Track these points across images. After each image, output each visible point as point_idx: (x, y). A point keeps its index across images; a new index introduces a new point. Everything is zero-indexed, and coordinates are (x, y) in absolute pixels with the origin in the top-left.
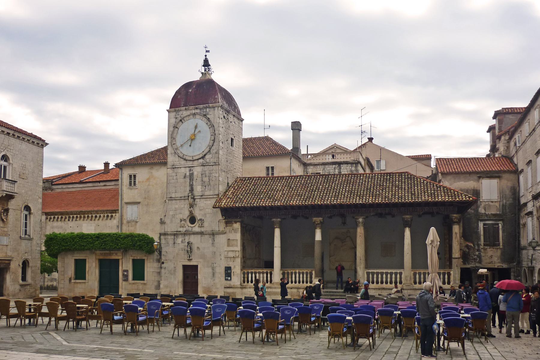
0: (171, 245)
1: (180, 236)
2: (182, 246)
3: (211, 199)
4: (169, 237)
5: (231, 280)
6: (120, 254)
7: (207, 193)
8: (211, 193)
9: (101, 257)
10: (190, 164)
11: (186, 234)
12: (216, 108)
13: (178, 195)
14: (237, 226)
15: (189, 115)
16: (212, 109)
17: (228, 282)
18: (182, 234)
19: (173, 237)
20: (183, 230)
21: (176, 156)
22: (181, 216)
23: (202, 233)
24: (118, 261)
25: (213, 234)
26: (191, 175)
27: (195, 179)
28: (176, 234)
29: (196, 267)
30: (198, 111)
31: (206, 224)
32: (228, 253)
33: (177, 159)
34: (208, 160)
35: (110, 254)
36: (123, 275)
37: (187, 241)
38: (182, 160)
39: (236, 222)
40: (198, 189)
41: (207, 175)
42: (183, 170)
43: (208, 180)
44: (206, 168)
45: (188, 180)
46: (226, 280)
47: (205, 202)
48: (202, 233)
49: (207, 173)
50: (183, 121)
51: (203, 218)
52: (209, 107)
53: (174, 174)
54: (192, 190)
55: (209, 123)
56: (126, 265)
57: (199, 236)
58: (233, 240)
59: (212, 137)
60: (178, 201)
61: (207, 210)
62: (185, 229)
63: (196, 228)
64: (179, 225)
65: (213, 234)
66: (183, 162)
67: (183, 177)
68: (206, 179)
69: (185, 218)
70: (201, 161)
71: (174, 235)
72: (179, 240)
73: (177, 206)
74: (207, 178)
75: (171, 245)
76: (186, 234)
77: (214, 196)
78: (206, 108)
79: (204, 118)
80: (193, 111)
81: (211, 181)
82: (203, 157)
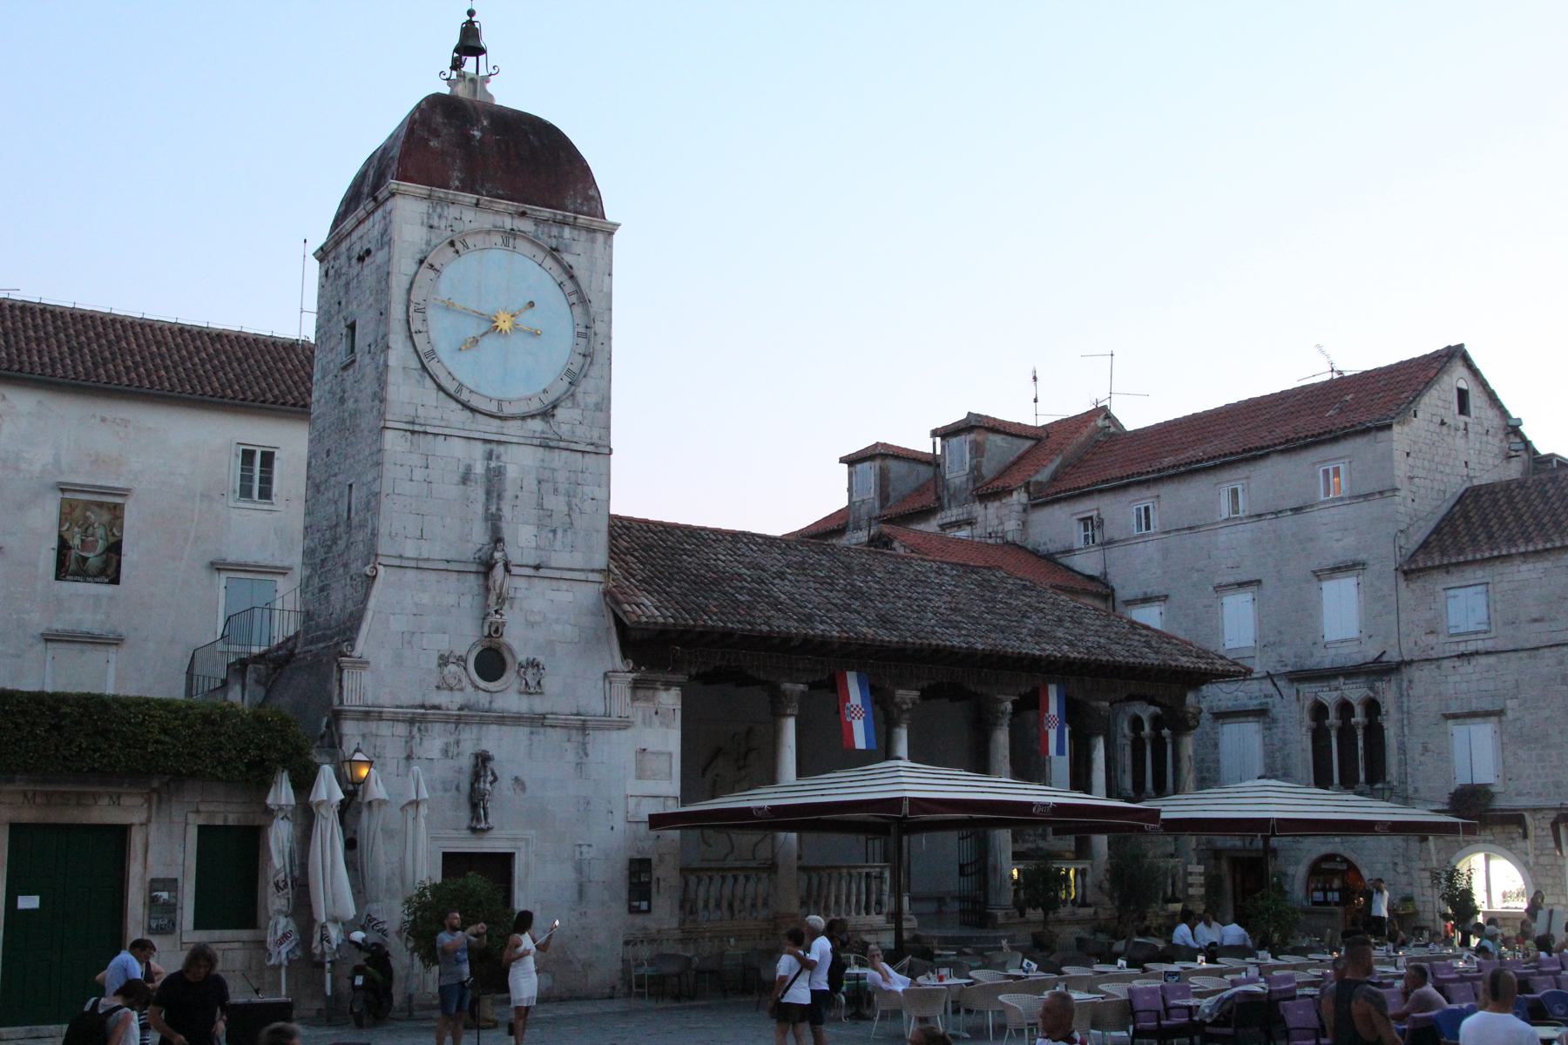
0: (391, 767)
1: (437, 726)
2: (444, 770)
3: (577, 586)
4: (384, 729)
5: (649, 911)
6: (138, 801)
7: (561, 558)
8: (577, 560)
9: (29, 815)
10: (489, 427)
11: (464, 718)
12: (600, 237)
13: (434, 550)
14: (670, 699)
15: (489, 232)
16: (584, 235)
17: (639, 920)
18: (446, 719)
19: (401, 729)
20: (449, 701)
21: (429, 382)
22: (443, 644)
23: (537, 721)
24: (121, 833)
25: (582, 726)
26: (494, 481)
27: (509, 494)
28: (418, 718)
29: (506, 860)
30: (526, 225)
31: (551, 683)
32: (638, 805)
33: (430, 395)
34: (565, 429)
35: (80, 800)
36: (153, 901)
37: (468, 748)
38: (454, 405)
39: (668, 685)
40: (522, 539)
41: (562, 488)
42: (458, 448)
43: (565, 509)
44: (559, 459)
45: (478, 492)
46: (633, 910)
47: (551, 595)
48: (537, 721)
49: (561, 477)
50: (459, 246)
51: (541, 659)
52: (574, 226)
53: (415, 459)
54: (497, 540)
55: (569, 287)
56: (163, 850)
57: (523, 732)
58: (658, 754)
59: (582, 341)
60: (432, 576)
61: (558, 627)
62: (458, 699)
63: (508, 696)
64: (434, 679)
65: (583, 728)
66: (457, 416)
67: (456, 478)
68: (557, 504)
69: (461, 650)
70: (537, 425)
71: (411, 721)
72: (434, 743)
73: (425, 598)
74: (562, 499)
75: (391, 767)
76: (464, 718)
77: (592, 576)
78: (563, 223)
79: (549, 262)
80: (508, 223)
81: (575, 515)
82: (547, 414)
